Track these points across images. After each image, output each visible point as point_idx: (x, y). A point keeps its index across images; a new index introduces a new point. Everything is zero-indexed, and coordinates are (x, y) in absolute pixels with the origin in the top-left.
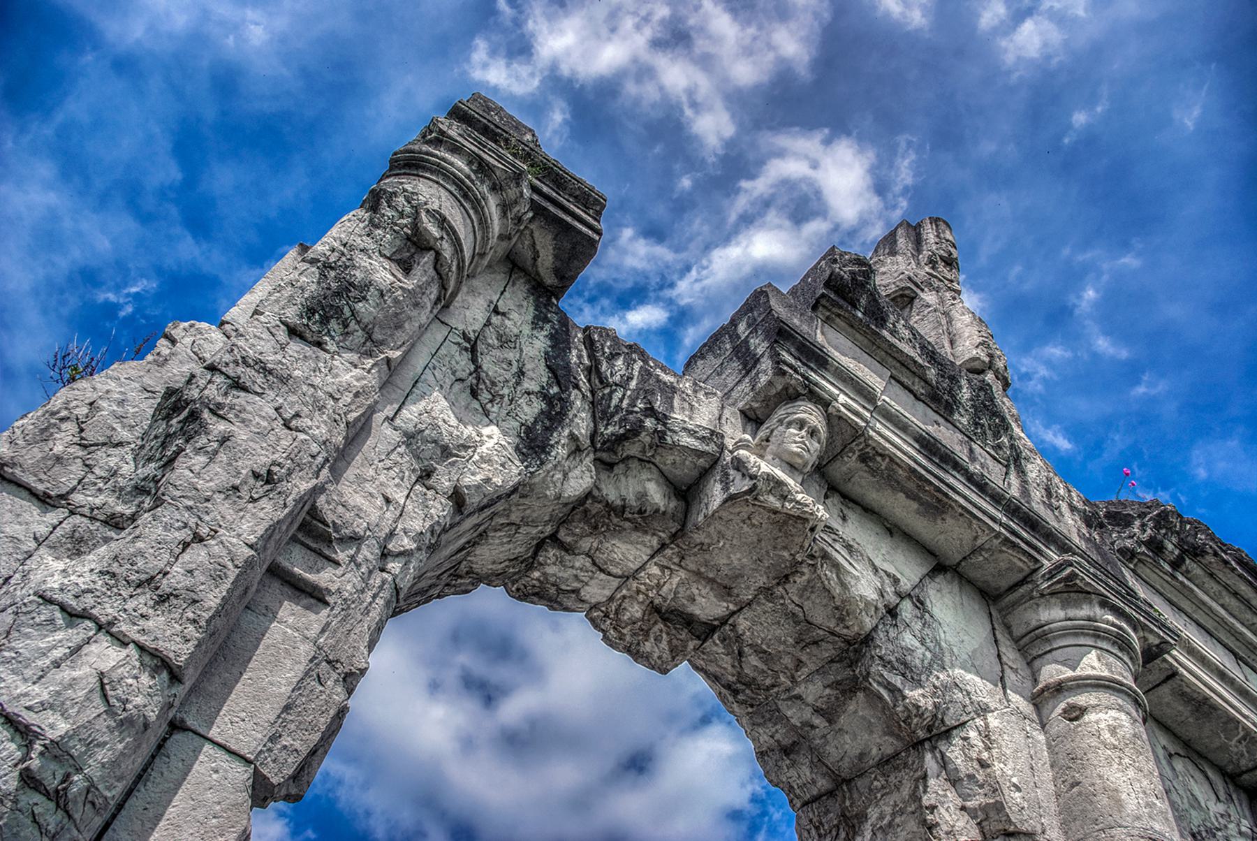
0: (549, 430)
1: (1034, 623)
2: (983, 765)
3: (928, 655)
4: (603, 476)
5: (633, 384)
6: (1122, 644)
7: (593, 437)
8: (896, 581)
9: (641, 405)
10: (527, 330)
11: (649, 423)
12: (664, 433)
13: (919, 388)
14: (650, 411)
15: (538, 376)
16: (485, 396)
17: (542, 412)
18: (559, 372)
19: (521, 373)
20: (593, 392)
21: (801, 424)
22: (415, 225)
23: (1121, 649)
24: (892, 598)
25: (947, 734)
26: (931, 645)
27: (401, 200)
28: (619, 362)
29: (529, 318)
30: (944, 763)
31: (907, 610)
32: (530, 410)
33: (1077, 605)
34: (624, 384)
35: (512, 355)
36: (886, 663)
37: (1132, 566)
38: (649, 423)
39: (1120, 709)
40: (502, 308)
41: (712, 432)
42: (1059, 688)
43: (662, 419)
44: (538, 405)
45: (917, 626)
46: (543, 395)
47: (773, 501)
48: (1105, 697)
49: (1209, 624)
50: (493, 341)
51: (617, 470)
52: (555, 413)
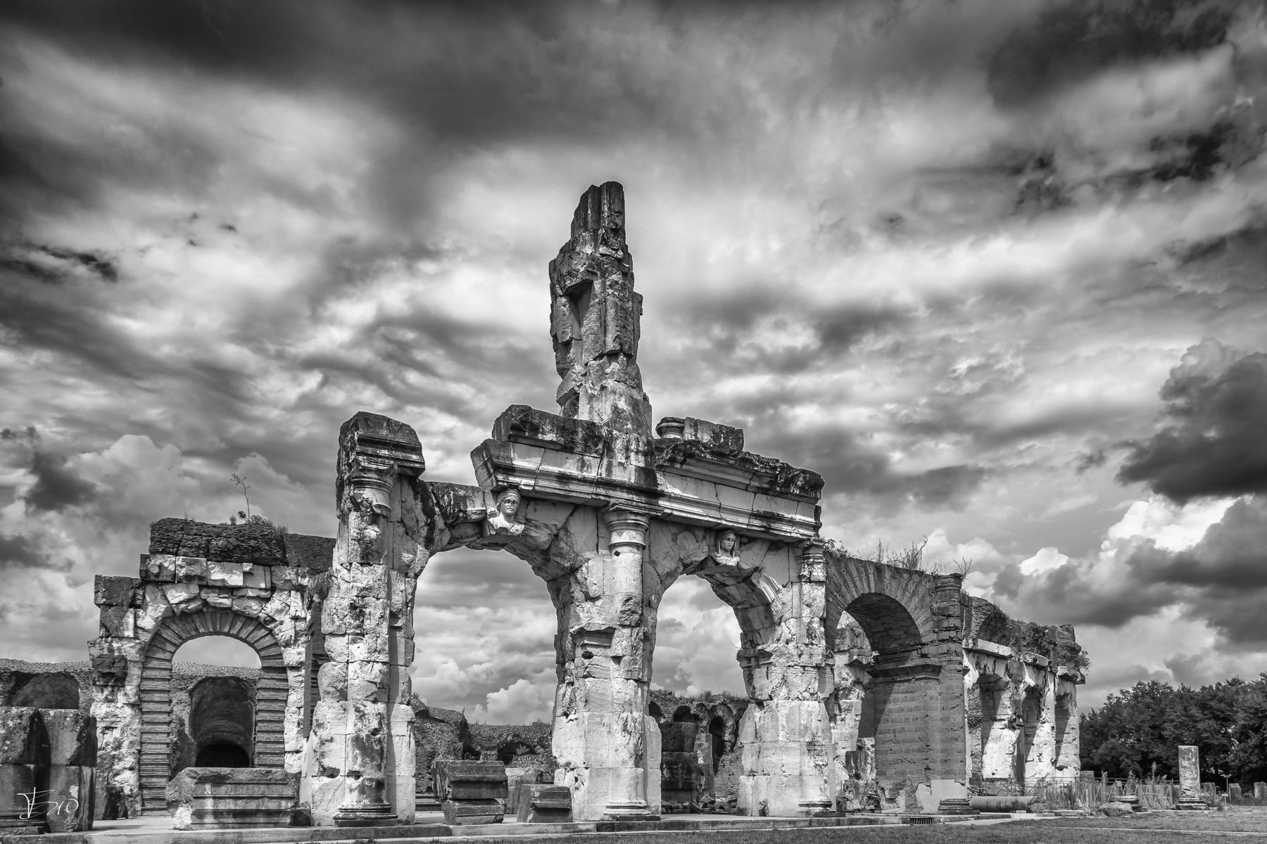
0: (432, 534)
2: (586, 579)
4: (453, 531)
5: (452, 503)
6: (637, 525)
7: (446, 524)
10: (413, 502)
11: (461, 515)
12: (466, 517)
13: (558, 447)
14: (460, 511)
15: (422, 518)
16: (410, 533)
18: (429, 513)
19: (417, 521)
20: (440, 510)
21: (509, 501)
22: (372, 510)
24: (555, 532)
25: (577, 570)
26: (569, 544)
27: (365, 502)
28: (446, 497)
29: (412, 496)
30: (576, 578)
31: (562, 533)
32: (424, 532)
33: (621, 515)
34: (449, 504)
35: (412, 515)
36: (554, 555)
38: (461, 515)
39: (631, 551)
40: (404, 500)
42: (615, 545)
43: (465, 512)
44: (426, 529)
45: (565, 538)
47: (504, 533)
50: (405, 512)
51: (457, 527)
52: (431, 526)
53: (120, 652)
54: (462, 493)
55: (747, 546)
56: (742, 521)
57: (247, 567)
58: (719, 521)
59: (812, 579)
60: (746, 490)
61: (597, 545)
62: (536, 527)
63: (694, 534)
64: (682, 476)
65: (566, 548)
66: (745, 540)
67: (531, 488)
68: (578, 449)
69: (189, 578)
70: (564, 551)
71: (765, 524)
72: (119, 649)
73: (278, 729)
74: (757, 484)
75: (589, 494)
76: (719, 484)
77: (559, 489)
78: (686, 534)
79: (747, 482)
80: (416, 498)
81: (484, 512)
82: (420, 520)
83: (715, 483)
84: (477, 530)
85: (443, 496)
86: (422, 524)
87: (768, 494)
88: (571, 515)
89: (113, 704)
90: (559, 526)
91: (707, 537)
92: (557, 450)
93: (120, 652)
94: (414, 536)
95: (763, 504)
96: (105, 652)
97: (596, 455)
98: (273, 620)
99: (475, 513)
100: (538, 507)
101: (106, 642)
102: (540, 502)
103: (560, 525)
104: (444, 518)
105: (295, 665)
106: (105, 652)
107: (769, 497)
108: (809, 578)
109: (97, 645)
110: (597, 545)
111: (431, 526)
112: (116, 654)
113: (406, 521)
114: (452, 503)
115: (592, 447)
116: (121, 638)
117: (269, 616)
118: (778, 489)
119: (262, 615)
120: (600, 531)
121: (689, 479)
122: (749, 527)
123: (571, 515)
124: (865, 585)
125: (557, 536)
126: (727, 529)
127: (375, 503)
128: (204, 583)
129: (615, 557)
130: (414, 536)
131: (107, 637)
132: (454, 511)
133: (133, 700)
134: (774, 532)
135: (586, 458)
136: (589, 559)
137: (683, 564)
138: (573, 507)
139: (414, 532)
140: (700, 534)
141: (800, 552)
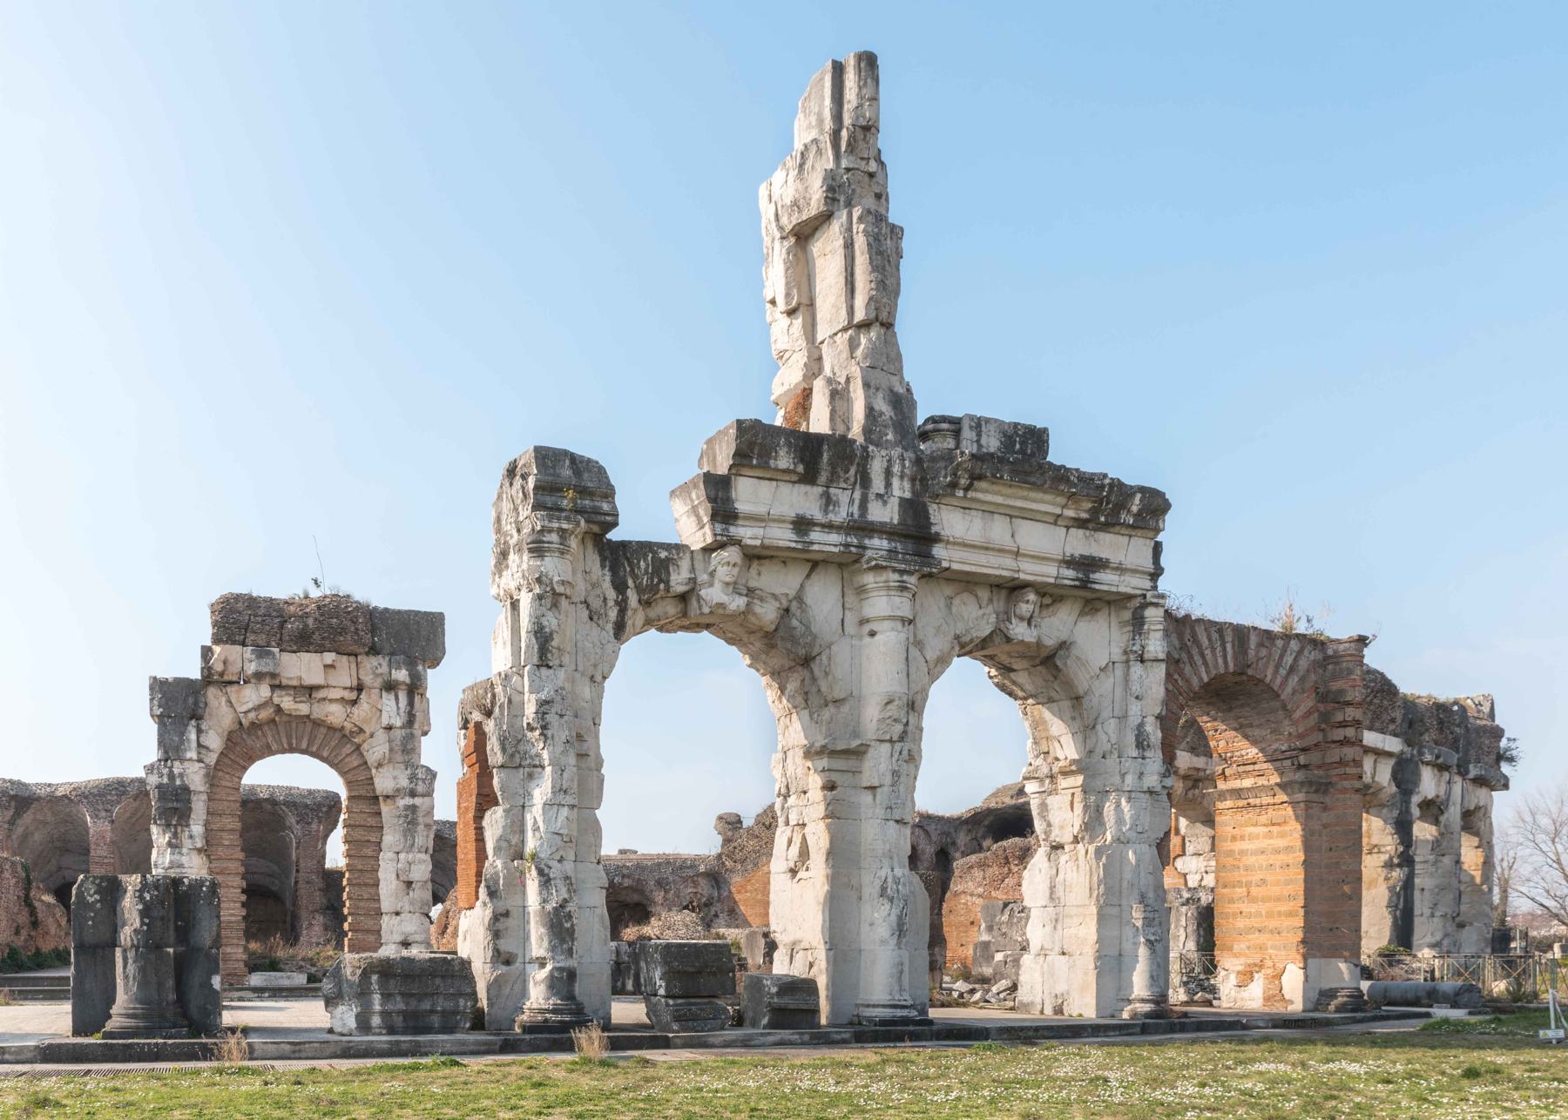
1: (861, 584)
3: (803, 628)
4: (648, 610)
8: (787, 595)
9: (656, 580)
15: (611, 594)
16: (595, 618)
19: (605, 599)
22: (553, 589)
24: (785, 604)
28: (642, 563)
31: (794, 604)
32: (613, 614)
39: (893, 629)
41: (690, 579)
47: (721, 611)
48: (887, 624)
52: (622, 606)
53: (182, 781)
54: (663, 554)
55: (1051, 609)
56: (1048, 573)
57: (329, 657)
58: (1016, 576)
59: (1146, 656)
60: (1055, 523)
61: (843, 620)
62: (761, 599)
63: (976, 596)
64: (964, 508)
65: (800, 629)
66: (1047, 600)
69: (259, 676)
70: (797, 633)
71: (1080, 576)
72: (181, 775)
73: (371, 882)
74: (1070, 513)
78: (966, 597)
80: (603, 567)
81: (693, 581)
82: (608, 598)
83: (1011, 517)
84: (680, 607)
85: (639, 562)
86: (611, 603)
87: (1087, 528)
88: (808, 576)
89: (177, 850)
90: (790, 597)
93: (182, 781)
94: (601, 622)
95: (1079, 543)
96: (165, 780)
98: (361, 731)
99: (681, 584)
100: (762, 569)
101: (165, 766)
103: (792, 593)
104: (638, 593)
105: (390, 793)
106: (165, 780)
107: (1088, 533)
108: (1141, 655)
109: (155, 771)
110: (843, 620)
111: (622, 606)
112: (178, 782)
113: (590, 600)
114: (650, 570)
116: (182, 760)
117: (356, 725)
118: (1103, 519)
119: (348, 725)
120: (846, 596)
121: (974, 513)
122: (1059, 581)
123: (808, 576)
124: (1220, 661)
125: (787, 610)
127: (556, 579)
128: (277, 682)
129: (867, 640)
130: (601, 622)
131: (166, 760)
132: (652, 581)
133: (199, 845)
136: (832, 644)
138: (810, 565)
140: (984, 594)
141: (1127, 615)
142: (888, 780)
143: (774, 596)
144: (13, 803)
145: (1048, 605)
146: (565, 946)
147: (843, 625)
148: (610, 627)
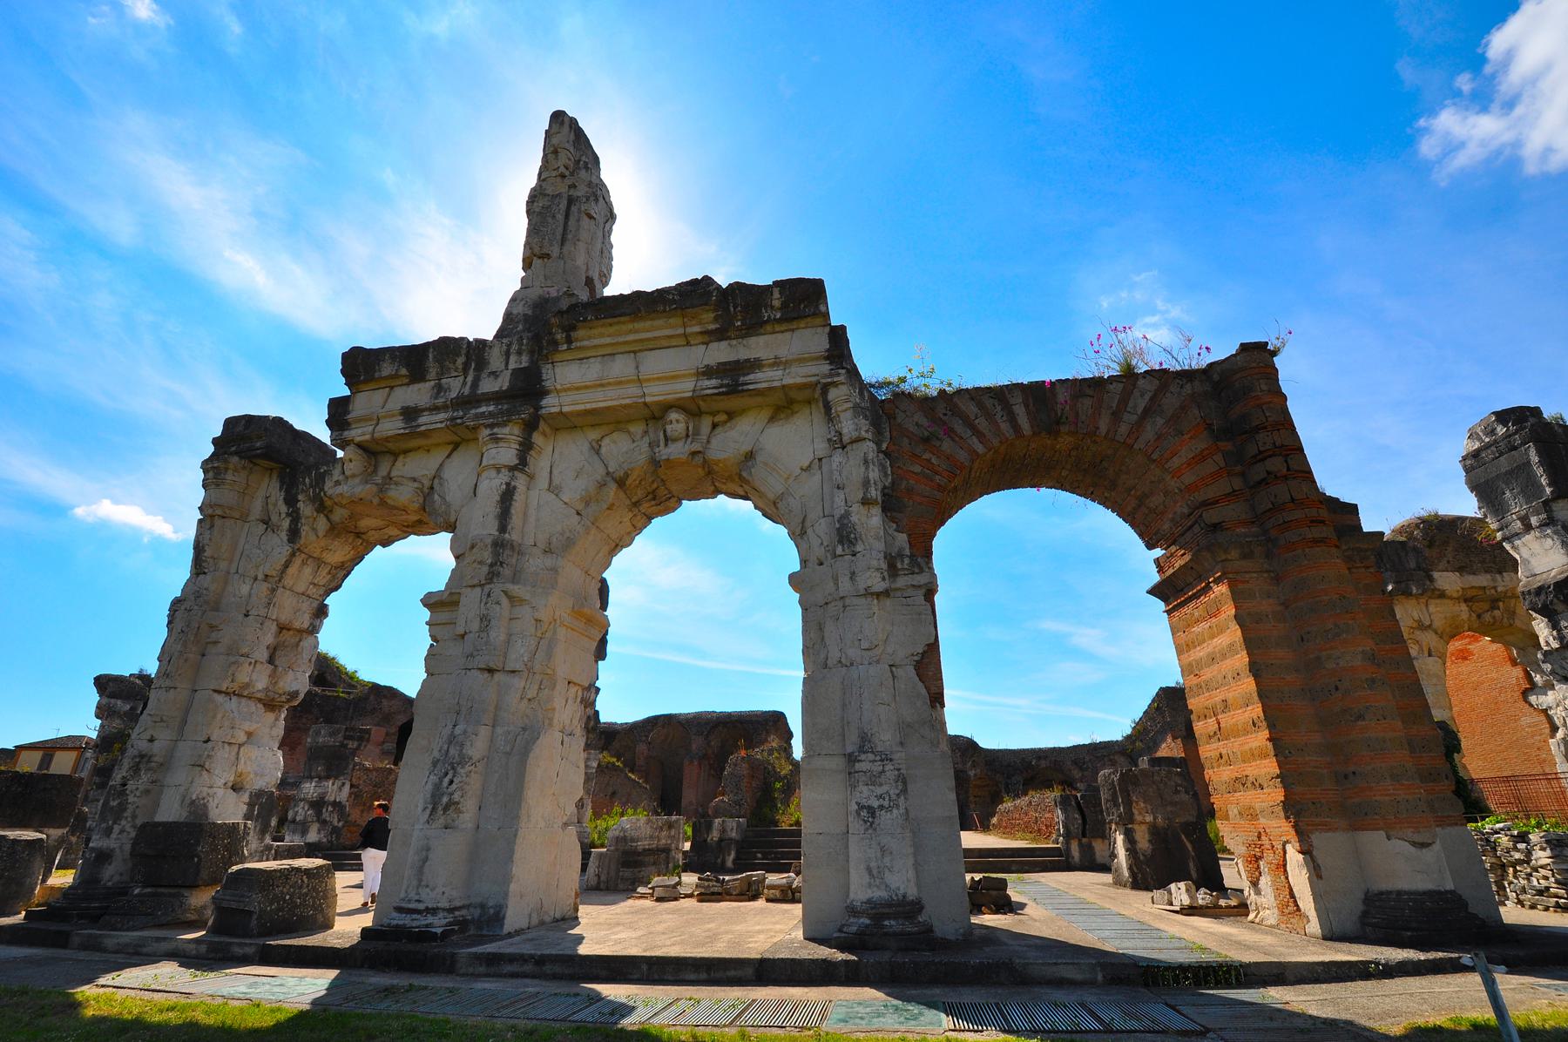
17: (291, 521)
19: (280, 513)
23: (497, 443)
28: (307, 480)
32: (286, 524)
37: (550, 361)
46: (288, 515)
49: (609, 350)
52: (295, 517)
55: (728, 424)
59: (845, 444)
62: (396, 484)
66: (722, 417)
67: (367, 437)
68: (433, 373)
75: (441, 422)
76: (640, 351)
77: (403, 428)
79: (681, 331)
80: (281, 490)
86: (283, 516)
91: (651, 430)
92: (408, 384)
97: (456, 374)
102: (411, 454)
111: (295, 517)
115: (451, 366)
123: (449, 456)
124: (1005, 427)
126: (667, 407)
134: (745, 387)
135: (444, 381)
137: (615, 480)
138: (450, 447)
139: (278, 527)
142: (475, 626)
143: (414, 480)
144: (603, 737)
145: (726, 422)
146: (104, 825)
147: (475, 489)
148: (284, 536)
